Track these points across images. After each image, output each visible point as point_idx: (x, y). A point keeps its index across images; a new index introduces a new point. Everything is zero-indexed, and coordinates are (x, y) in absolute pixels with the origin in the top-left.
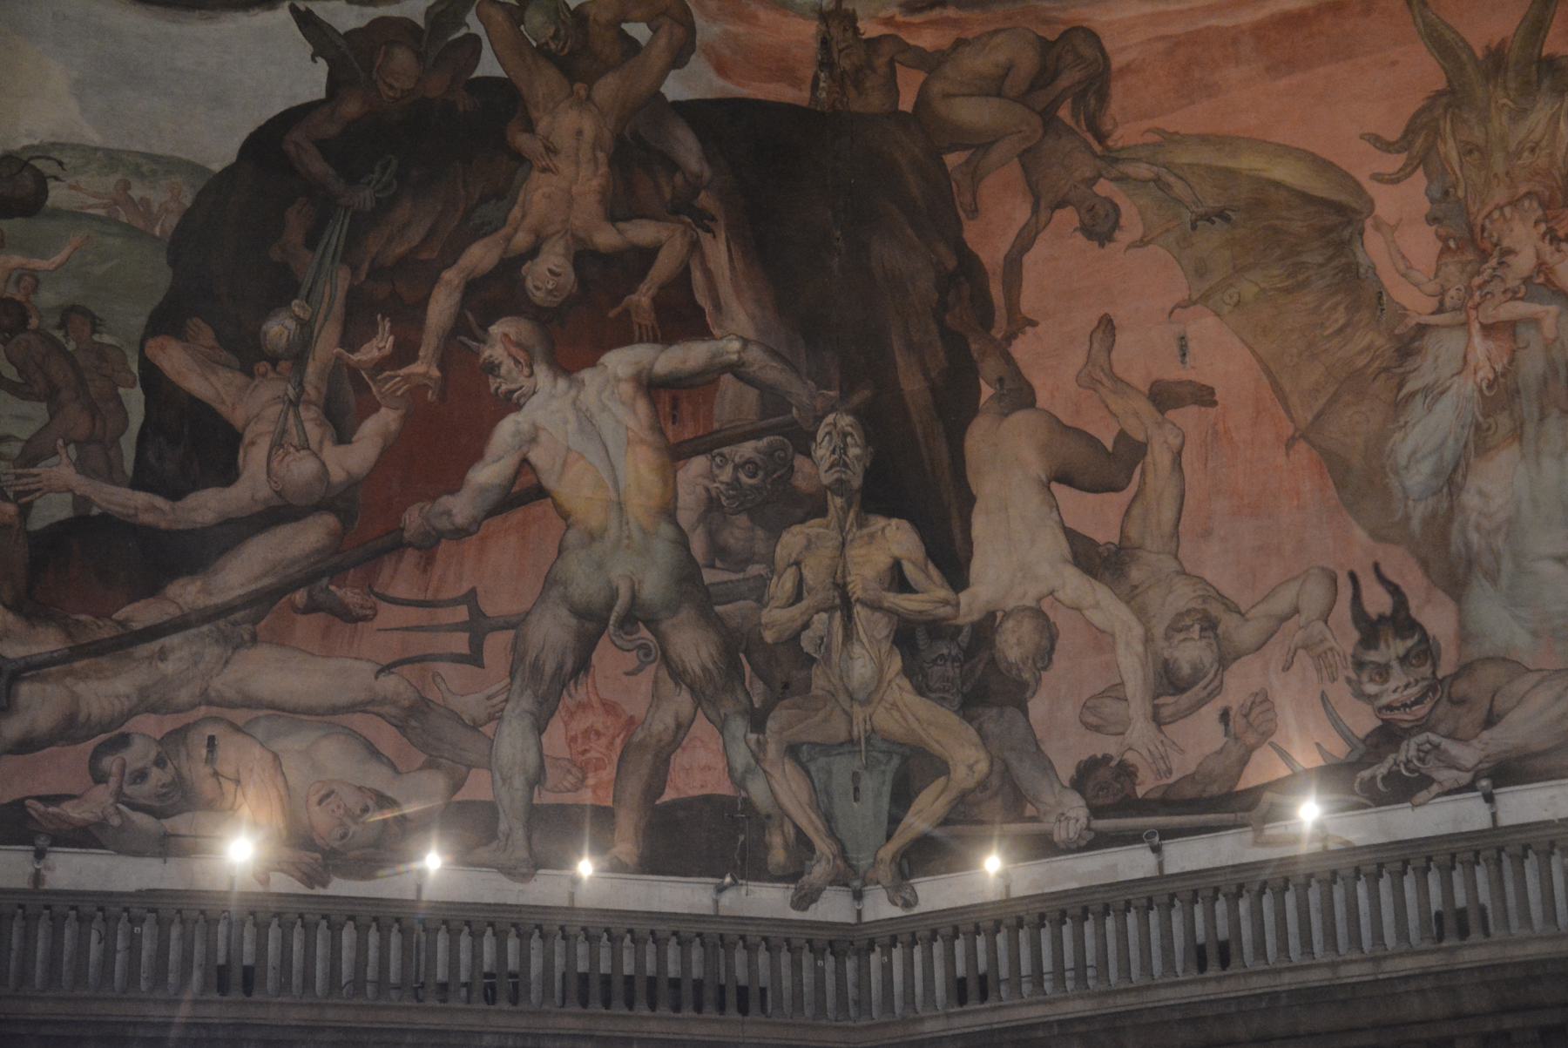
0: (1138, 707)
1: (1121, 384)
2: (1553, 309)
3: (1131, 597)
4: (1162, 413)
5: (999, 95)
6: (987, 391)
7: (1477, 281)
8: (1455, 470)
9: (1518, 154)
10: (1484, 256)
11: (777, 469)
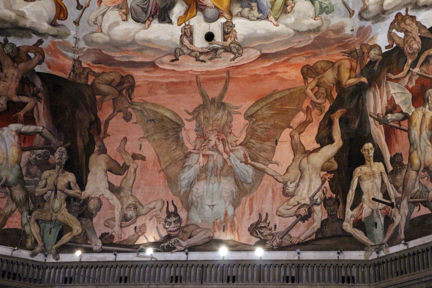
0: (117, 223)
1: (126, 153)
2: (216, 154)
3: (120, 199)
4: (134, 160)
5: (110, 85)
6: (96, 148)
7: (203, 145)
8: (192, 183)
9: (215, 121)
10: (205, 140)
11: (46, 157)
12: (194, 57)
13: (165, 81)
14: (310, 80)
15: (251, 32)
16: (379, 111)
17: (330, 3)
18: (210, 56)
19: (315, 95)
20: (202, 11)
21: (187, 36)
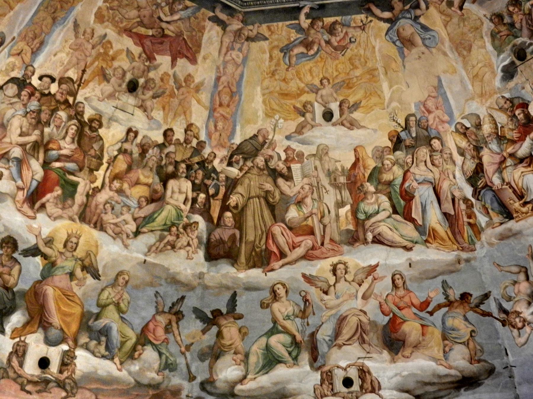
12: (20, 384)
15: (93, 370)
17: (175, 361)
18: (38, 388)
20: (45, 329)
21: (18, 355)
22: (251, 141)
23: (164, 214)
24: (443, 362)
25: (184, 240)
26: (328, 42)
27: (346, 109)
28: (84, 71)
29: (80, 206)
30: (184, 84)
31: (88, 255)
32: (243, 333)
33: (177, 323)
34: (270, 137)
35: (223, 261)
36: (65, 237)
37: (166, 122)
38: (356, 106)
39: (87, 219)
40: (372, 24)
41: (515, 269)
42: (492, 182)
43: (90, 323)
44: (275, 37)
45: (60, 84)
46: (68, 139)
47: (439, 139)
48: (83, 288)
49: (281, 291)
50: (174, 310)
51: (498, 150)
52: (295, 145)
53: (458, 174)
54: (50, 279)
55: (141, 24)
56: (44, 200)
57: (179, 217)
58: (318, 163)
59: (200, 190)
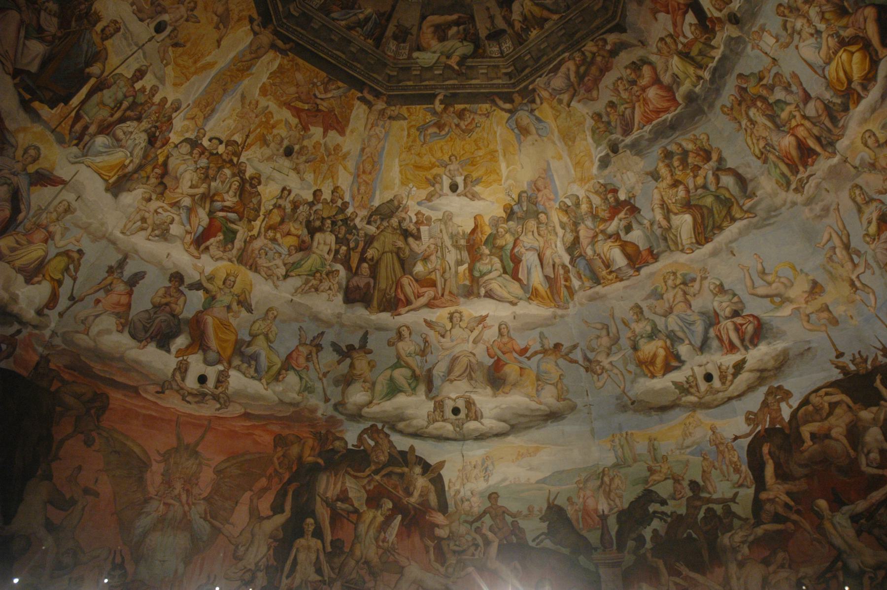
2: (178, 504)
10: (170, 488)
13: (144, 411)
14: (279, 449)
16: (329, 494)
18: (197, 399)
19: (279, 464)
22: (388, 204)
23: (310, 261)
24: (535, 399)
25: (326, 285)
26: (457, 126)
27: (469, 183)
28: (248, 136)
29: (238, 250)
30: (333, 152)
31: (243, 292)
32: (372, 365)
33: (317, 354)
34: (404, 202)
35: (358, 304)
36: (225, 276)
37: (315, 183)
38: (478, 181)
39: (244, 262)
40: (495, 113)
41: (599, 326)
42: (585, 253)
43: (243, 349)
44: (413, 118)
45: (227, 146)
46: (231, 193)
47: (545, 214)
48: (238, 319)
49: (405, 333)
50: (314, 343)
51: (592, 227)
52: (426, 212)
53: (559, 244)
54: (211, 309)
55: (299, 99)
56: (208, 243)
57: (323, 265)
58: (443, 227)
59: (342, 243)
